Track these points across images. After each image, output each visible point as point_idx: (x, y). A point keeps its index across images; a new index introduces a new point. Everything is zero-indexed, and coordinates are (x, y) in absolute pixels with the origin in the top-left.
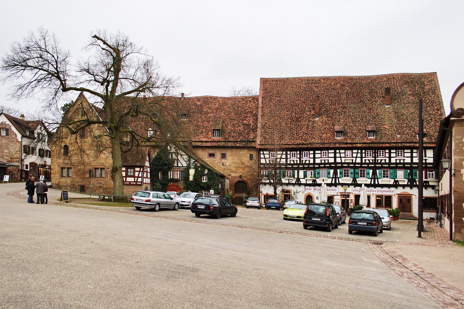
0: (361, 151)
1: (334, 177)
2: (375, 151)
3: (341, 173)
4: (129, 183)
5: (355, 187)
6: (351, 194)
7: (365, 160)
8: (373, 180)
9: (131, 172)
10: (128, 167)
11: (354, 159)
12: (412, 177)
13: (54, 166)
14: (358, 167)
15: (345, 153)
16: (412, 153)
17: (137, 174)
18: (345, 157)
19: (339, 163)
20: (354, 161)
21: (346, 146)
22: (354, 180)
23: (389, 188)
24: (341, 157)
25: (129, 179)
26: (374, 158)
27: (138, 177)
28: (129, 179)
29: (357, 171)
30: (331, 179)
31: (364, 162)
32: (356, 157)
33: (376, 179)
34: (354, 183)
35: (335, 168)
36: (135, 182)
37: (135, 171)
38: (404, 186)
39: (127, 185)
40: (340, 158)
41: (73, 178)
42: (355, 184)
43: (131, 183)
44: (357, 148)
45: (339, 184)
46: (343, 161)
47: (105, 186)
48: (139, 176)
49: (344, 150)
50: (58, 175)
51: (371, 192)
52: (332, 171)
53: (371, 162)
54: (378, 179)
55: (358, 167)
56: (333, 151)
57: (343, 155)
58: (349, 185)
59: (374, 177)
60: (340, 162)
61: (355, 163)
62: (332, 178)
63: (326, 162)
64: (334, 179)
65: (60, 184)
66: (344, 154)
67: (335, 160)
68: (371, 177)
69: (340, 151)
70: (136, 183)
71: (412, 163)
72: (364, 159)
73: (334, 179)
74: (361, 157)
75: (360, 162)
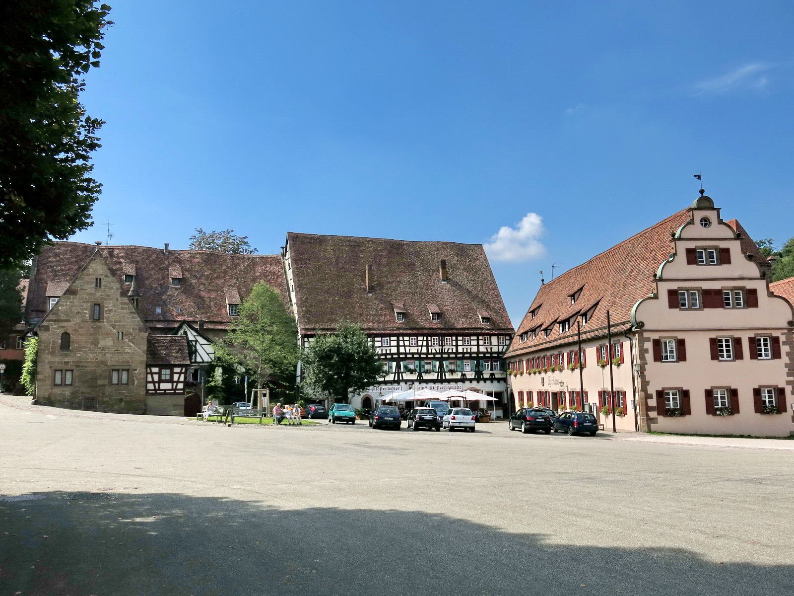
0: (427, 338)
2: (442, 338)
4: (163, 392)
5: (420, 383)
7: (431, 350)
9: (166, 374)
10: (161, 367)
11: (420, 348)
12: (479, 369)
14: (423, 359)
15: (409, 341)
16: (478, 340)
17: (176, 377)
18: (409, 346)
19: (402, 354)
20: (419, 352)
21: (411, 332)
22: (420, 375)
24: (405, 346)
25: (164, 386)
27: (178, 382)
28: (164, 386)
29: (423, 363)
30: (394, 374)
31: (430, 352)
32: (422, 346)
34: (420, 378)
35: (398, 360)
37: (172, 374)
39: (161, 394)
43: (167, 392)
44: (423, 335)
45: (403, 380)
46: (408, 351)
47: (128, 399)
52: (394, 364)
53: (438, 351)
54: (445, 372)
55: (423, 359)
56: (395, 338)
57: (407, 343)
58: (413, 381)
59: (441, 370)
61: (420, 354)
62: (395, 373)
63: (388, 352)
65: (53, 399)
67: (398, 350)
68: (437, 371)
71: (478, 352)
72: (430, 348)
74: (427, 346)
75: (426, 352)
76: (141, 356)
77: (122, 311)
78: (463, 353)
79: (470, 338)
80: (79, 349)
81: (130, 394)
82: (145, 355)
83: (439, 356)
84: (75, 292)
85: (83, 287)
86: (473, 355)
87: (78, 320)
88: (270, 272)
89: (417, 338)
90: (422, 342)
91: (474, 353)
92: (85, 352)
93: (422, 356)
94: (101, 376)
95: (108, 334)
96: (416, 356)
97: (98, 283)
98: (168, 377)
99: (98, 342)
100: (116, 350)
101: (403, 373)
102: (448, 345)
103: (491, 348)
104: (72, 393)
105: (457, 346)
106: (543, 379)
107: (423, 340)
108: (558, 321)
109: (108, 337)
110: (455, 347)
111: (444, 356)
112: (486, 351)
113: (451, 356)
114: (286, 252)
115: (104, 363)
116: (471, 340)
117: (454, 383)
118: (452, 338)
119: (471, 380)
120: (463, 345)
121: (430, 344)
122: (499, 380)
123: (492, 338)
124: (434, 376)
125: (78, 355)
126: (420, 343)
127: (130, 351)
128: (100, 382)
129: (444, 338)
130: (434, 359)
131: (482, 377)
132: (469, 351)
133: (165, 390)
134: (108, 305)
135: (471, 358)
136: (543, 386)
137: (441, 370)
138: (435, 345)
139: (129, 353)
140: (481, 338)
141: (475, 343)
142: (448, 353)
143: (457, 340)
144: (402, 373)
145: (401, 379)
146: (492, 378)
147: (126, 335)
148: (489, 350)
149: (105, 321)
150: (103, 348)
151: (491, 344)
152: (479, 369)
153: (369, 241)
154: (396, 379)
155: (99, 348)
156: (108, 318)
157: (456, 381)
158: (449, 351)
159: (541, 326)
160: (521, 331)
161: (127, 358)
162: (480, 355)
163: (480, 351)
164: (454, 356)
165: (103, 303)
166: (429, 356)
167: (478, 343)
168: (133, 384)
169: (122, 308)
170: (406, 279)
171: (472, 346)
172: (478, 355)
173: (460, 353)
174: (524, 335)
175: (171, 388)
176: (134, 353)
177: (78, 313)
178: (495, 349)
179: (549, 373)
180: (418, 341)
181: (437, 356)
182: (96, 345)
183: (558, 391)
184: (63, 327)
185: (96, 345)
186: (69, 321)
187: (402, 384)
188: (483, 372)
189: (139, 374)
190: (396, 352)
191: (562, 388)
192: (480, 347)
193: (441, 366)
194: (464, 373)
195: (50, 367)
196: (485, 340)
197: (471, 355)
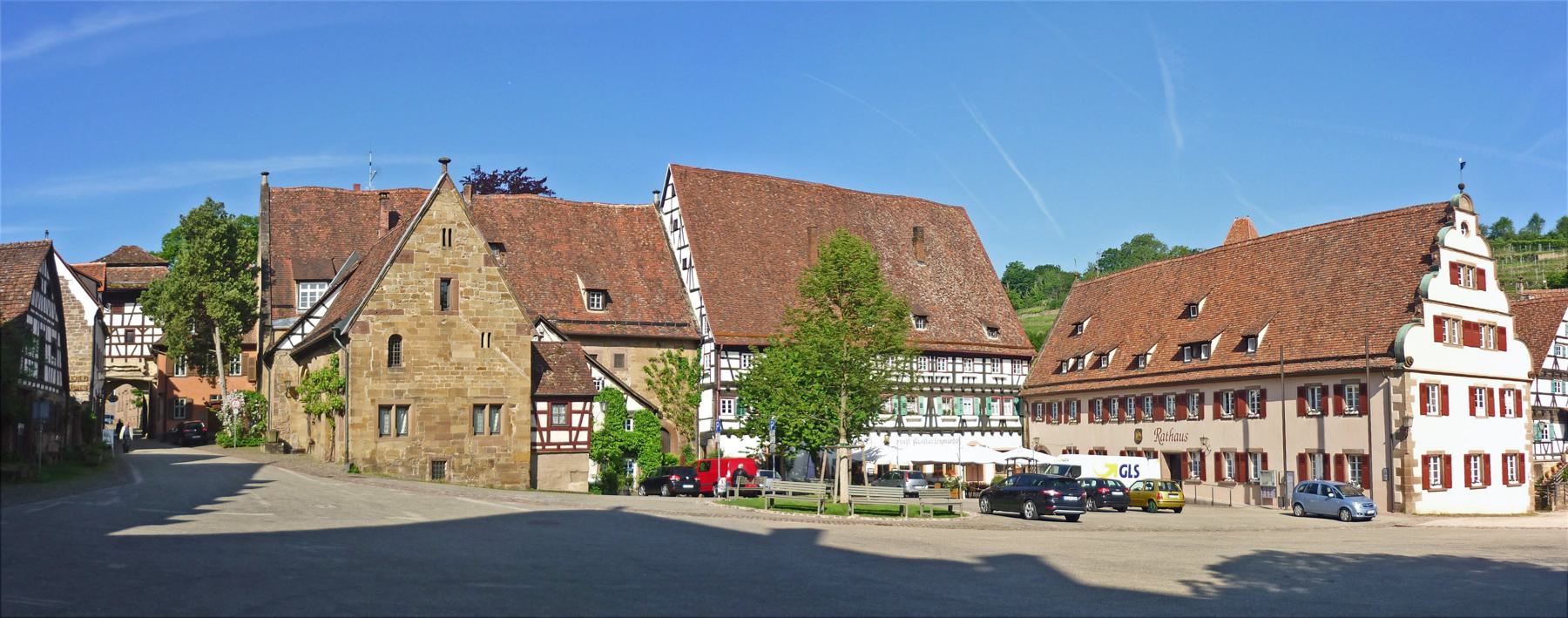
4: (555, 447)
9: (560, 415)
13: (361, 402)
17: (575, 419)
27: (579, 429)
29: (904, 399)
34: (900, 425)
36: (570, 443)
37: (570, 412)
41: (414, 439)
43: (562, 447)
47: (502, 461)
48: (583, 425)
50: (371, 430)
59: (931, 412)
70: (575, 448)
76: (522, 379)
77: (491, 292)
80: (419, 366)
81: (506, 451)
82: (529, 378)
84: (408, 256)
85: (422, 247)
87: (415, 311)
88: (640, 234)
92: (428, 372)
94: (456, 418)
95: (466, 337)
97: (447, 238)
98: (562, 420)
99: (450, 354)
100: (480, 369)
104: (410, 451)
105: (954, 372)
109: (467, 344)
114: (664, 199)
115: (460, 392)
116: (974, 364)
119: (972, 431)
122: (1011, 431)
125: (418, 378)
127: (503, 370)
128: (455, 430)
131: (988, 425)
133: (559, 444)
134: (465, 281)
135: (973, 393)
137: (930, 413)
139: (502, 373)
146: (1003, 429)
147: (496, 338)
149: (460, 311)
150: (459, 364)
151: (1002, 373)
152: (984, 411)
153: (798, 186)
155: (452, 364)
156: (466, 305)
157: (951, 431)
161: (499, 383)
165: (456, 277)
168: (510, 432)
169: (490, 288)
171: (972, 371)
175: (568, 441)
176: (509, 374)
177: (415, 296)
178: (1007, 382)
182: (446, 359)
184: (391, 324)
185: (446, 359)
186: (400, 312)
188: (990, 418)
189: (519, 413)
192: (987, 375)
193: (930, 406)
194: (963, 417)
195: (373, 401)
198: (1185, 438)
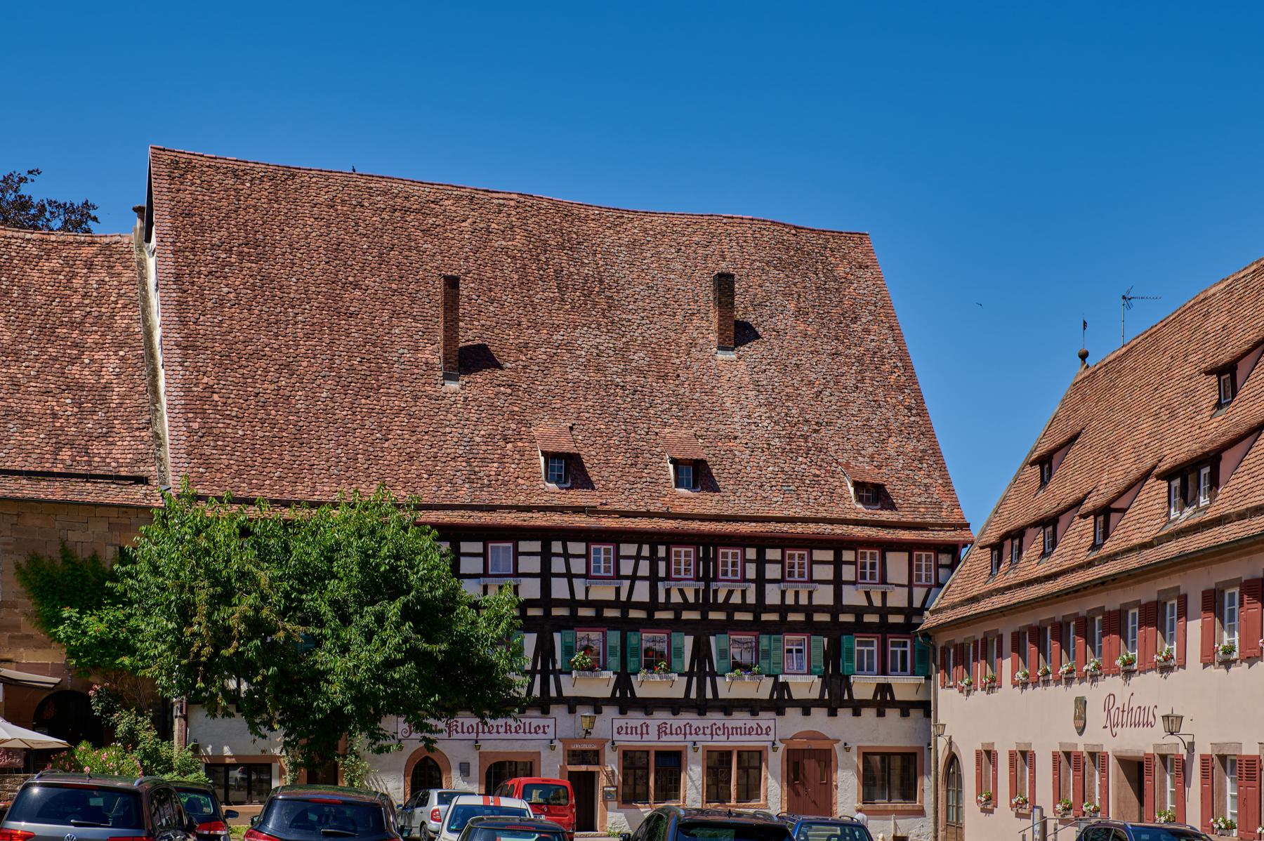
0: (654, 551)
1: (539, 667)
2: (706, 552)
3: (569, 651)
5: (623, 712)
6: (608, 745)
7: (668, 592)
8: (695, 679)
14: (637, 625)
15: (587, 556)
18: (587, 576)
19: (560, 603)
20: (623, 597)
22: (623, 682)
23: (754, 713)
24: (569, 576)
26: (702, 585)
31: (662, 599)
32: (634, 578)
33: (708, 679)
34: (623, 694)
38: (806, 707)
40: (565, 580)
42: (625, 700)
45: (561, 699)
49: (584, 545)
51: (685, 734)
53: (691, 599)
54: (714, 675)
56: (536, 546)
57: (578, 566)
58: (597, 704)
59: (702, 668)
60: (568, 597)
61: (629, 605)
64: (538, 677)
66: (584, 560)
67: (546, 588)
68: (687, 669)
69: (565, 547)
73: (538, 677)
74: (653, 579)
78: (783, 609)
79: (811, 555)
83: (694, 615)
86: (818, 617)
89: (617, 550)
90: (632, 562)
91: (822, 609)
93: (634, 614)
96: (609, 613)
101: (561, 672)
102: (730, 576)
103: (884, 595)
105: (761, 581)
106: (1081, 703)
107: (638, 558)
108: (1157, 471)
110: (753, 586)
111: (713, 616)
112: (865, 603)
113: (739, 616)
117: (747, 715)
118: (744, 554)
120: (782, 580)
121: (662, 573)
123: (891, 557)
124: (674, 687)
126: (626, 568)
129: (716, 553)
130: (677, 625)
131: (846, 697)
132: (803, 601)
135: (810, 627)
136: (1081, 731)
137: (702, 667)
138: (683, 575)
140: (848, 555)
141: (826, 572)
142: (728, 607)
143: (761, 562)
144: (556, 673)
145: (553, 693)
148: (877, 602)
151: (884, 581)
154: (536, 692)
158: (731, 601)
159: (1080, 502)
160: (992, 537)
162: (844, 618)
163: (845, 602)
164: (748, 617)
166: (659, 615)
167: (838, 573)
170: (587, 340)
172: (835, 617)
173: (772, 609)
174: (1008, 544)
178: (897, 598)
179: (1112, 684)
180: (618, 558)
181: (686, 615)
183: (1150, 751)
187: (558, 711)
190: (537, 595)
191: (1174, 739)
192: (845, 588)
194: (781, 679)
196: (864, 567)
197: (809, 617)
198: (1151, 719)
